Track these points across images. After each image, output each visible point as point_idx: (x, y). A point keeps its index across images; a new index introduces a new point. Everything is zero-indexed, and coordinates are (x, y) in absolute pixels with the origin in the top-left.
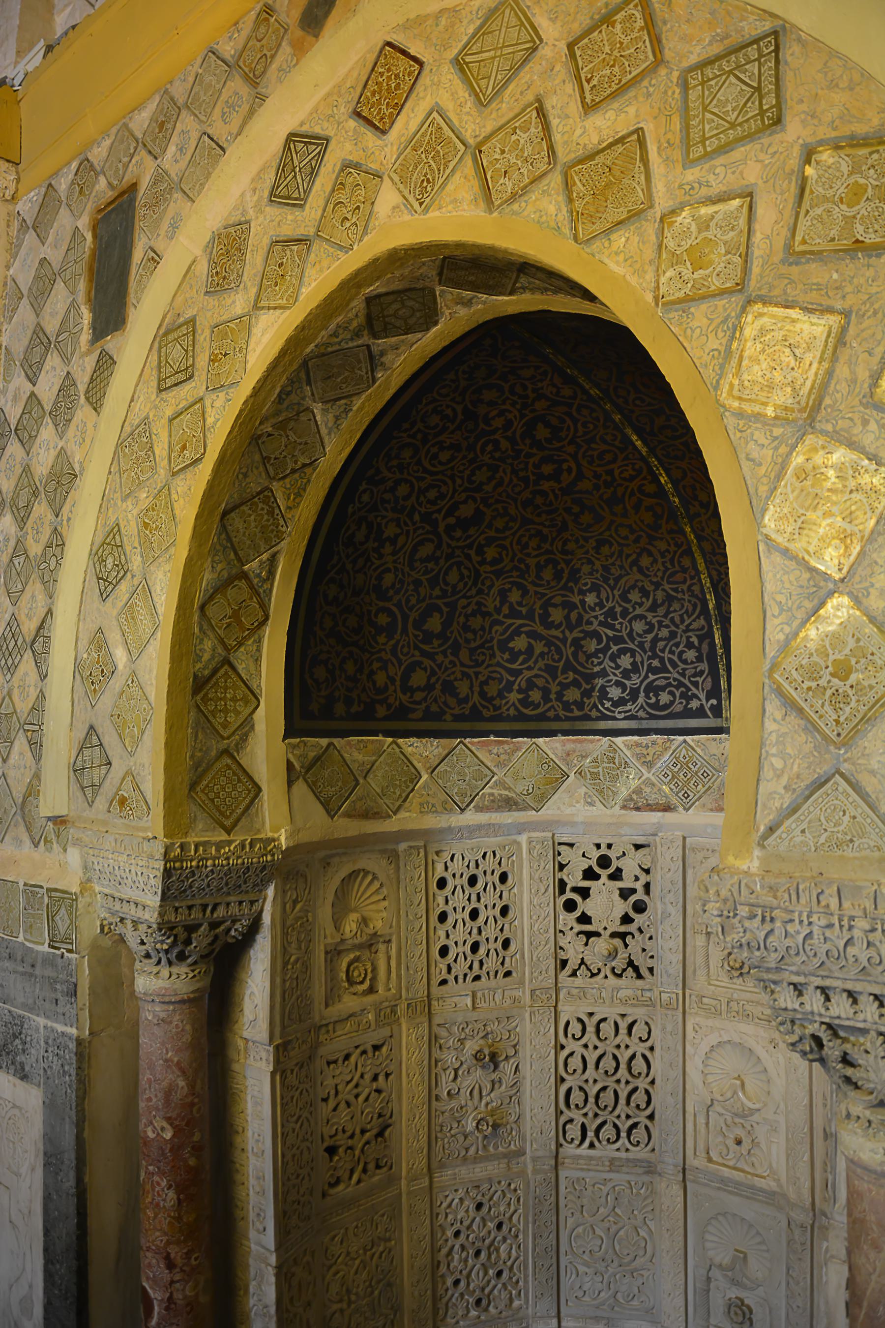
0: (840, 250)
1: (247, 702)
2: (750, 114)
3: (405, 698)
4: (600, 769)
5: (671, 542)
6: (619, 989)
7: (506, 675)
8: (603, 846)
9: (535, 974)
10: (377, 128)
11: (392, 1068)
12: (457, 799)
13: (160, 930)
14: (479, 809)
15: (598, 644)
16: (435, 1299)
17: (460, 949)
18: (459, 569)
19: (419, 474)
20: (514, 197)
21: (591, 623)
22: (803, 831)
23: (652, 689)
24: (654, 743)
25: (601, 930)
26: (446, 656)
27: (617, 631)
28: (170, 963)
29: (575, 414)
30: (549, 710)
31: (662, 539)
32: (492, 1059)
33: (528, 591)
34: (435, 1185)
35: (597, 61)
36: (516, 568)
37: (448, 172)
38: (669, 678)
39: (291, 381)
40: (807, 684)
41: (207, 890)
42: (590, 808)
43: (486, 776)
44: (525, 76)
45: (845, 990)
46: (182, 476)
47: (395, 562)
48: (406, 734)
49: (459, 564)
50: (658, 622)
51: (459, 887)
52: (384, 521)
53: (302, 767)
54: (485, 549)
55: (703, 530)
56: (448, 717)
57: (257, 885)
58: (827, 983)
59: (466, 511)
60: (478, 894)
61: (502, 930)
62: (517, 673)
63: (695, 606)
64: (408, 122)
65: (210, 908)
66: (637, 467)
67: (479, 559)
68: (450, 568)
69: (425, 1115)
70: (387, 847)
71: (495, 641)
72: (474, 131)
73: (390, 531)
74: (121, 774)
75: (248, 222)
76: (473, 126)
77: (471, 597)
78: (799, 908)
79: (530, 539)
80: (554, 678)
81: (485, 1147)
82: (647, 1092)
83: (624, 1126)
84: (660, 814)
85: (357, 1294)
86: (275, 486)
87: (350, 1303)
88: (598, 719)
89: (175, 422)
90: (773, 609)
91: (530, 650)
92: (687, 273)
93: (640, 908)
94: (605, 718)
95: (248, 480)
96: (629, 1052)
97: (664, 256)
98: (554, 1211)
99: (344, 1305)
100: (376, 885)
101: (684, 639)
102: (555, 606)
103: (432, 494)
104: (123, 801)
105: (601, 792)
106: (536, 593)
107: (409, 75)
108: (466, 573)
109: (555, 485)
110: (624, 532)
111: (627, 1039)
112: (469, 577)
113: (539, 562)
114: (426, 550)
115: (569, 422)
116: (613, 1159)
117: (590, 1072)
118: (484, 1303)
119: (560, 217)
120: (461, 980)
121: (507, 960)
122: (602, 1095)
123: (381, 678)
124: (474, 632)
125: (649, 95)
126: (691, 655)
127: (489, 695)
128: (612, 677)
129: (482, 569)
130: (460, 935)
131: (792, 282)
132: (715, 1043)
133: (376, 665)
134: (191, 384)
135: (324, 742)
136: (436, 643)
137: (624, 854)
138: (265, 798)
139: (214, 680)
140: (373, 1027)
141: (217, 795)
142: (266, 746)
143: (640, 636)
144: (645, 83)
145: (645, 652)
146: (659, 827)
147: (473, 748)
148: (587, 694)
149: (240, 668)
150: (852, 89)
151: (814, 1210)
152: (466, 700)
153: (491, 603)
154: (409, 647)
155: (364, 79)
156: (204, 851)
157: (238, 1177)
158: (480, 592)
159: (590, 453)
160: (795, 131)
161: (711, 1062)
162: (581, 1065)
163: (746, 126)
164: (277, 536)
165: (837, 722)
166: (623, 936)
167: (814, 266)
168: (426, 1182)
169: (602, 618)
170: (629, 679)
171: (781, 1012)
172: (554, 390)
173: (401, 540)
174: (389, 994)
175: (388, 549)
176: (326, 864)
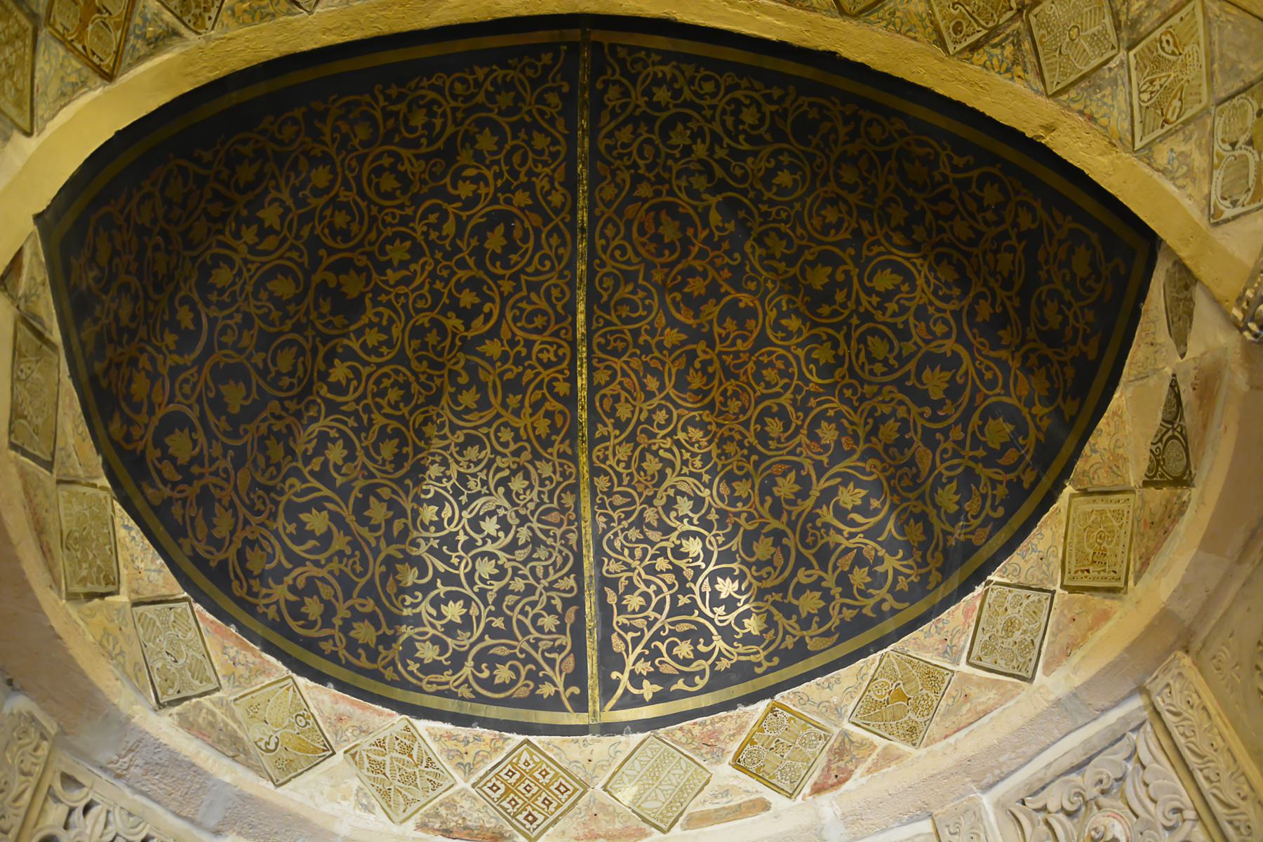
4: (387, 758)
5: (558, 469)
14: (187, 724)
15: (421, 576)
18: (296, 358)
19: (350, 176)
21: (418, 546)
23: (484, 657)
24: (477, 738)
26: (225, 456)
27: (452, 566)
29: (543, 236)
31: (548, 461)
33: (355, 458)
38: (514, 647)
42: (366, 815)
49: (301, 352)
50: (513, 568)
55: (604, 460)
56: (186, 543)
59: (353, 286)
62: (298, 561)
63: (566, 559)
66: (560, 352)
68: (290, 343)
71: (284, 499)
73: (270, 215)
79: (393, 386)
80: (348, 596)
88: (393, 683)
91: (326, 539)
94: (404, 684)
101: (544, 598)
102: (380, 499)
103: (341, 219)
105: (385, 794)
106: (364, 467)
108: (300, 372)
109: (462, 328)
110: (506, 435)
113: (386, 426)
114: (283, 288)
115: (531, 244)
124: (268, 459)
126: (549, 622)
127: (249, 566)
148: (387, 641)
152: (218, 544)
153: (304, 441)
154: (193, 389)
159: (523, 305)
169: (435, 544)
170: (454, 637)
172: (547, 187)
173: (270, 243)
175: (249, 235)
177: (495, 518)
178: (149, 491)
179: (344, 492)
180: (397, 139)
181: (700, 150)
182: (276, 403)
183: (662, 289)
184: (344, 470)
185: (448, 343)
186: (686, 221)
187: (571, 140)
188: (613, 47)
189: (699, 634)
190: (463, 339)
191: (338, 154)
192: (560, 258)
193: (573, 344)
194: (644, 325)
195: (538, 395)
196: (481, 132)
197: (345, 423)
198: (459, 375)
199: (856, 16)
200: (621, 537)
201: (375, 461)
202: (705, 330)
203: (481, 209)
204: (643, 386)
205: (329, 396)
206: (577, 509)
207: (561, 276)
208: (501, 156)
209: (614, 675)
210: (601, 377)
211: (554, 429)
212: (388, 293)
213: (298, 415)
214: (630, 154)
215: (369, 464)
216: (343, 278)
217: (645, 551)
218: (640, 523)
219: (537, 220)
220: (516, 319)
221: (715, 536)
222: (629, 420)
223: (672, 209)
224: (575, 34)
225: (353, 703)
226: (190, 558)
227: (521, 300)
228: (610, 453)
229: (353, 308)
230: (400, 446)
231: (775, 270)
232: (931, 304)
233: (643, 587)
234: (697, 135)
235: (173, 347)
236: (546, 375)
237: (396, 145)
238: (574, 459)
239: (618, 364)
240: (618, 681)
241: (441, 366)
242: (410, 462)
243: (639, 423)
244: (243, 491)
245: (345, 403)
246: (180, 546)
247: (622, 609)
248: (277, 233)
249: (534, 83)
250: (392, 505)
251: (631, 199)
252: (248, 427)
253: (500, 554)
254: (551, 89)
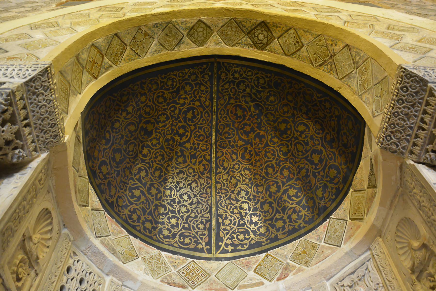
5: (206, 181)
7: (127, 202)
18: (134, 147)
19: (151, 98)
26: (114, 173)
30: (138, 226)
31: (203, 179)
47: (123, 121)
49: (135, 145)
55: (219, 179)
59: (150, 127)
62: (131, 203)
66: (207, 147)
68: (133, 143)
71: (129, 186)
73: (130, 109)
79: (159, 155)
100: (49, 236)
102: (154, 187)
103: (148, 110)
106: (150, 178)
108: (135, 149)
109: (179, 139)
110: (191, 171)
113: (157, 167)
114: (132, 128)
115: (199, 116)
124: (125, 174)
128: (166, 226)
129: (139, 154)
152: (112, 197)
153: (135, 170)
154: (108, 154)
159: (197, 133)
169: (169, 201)
172: (205, 100)
173: (129, 116)
175: (124, 114)
177: (187, 195)
178: (97, 181)
179: (145, 185)
180: (164, 88)
181: (248, 90)
182: (128, 159)
183: (238, 129)
184: (145, 179)
186: (244, 110)
187: (211, 87)
188: (223, 63)
189: (246, 232)
190: (180, 142)
191: (148, 92)
192: (208, 120)
193: (211, 145)
194: (232, 139)
195: (201, 159)
196: (186, 86)
197: (146, 165)
198: (178, 153)
199: (289, 56)
201: (154, 177)
202: (250, 141)
203: (186, 106)
204: (232, 157)
205: (142, 158)
206: (211, 194)
207: (208, 125)
208: (192, 92)
209: (220, 243)
210: (220, 154)
211: (205, 169)
212: (159, 129)
213: (133, 163)
214: (228, 91)
215: (152, 178)
216: (147, 125)
219: (201, 109)
220: (195, 137)
221: (252, 203)
222: (227, 167)
223: (240, 106)
224: (213, 60)
227: (196, 132)
228: (221, 177)
229: (150, 133)
230: (160, 173)
231: (270, 124)
232: (314, 135)
234: (247, 86)
235: (104, 143)
236: (203, 153)
237: (164, 90)
238: (211, 179)
239: (224, 151)
241: (173, 150)
243: (230, 168)
244: (118, 183)
245: (146, 160)
246: (103, 196)
248: (131, 114)
249: (201, 73)
250: (158, 189)
251: (228, 104)
252: (121, 165)
254: (206, 74)
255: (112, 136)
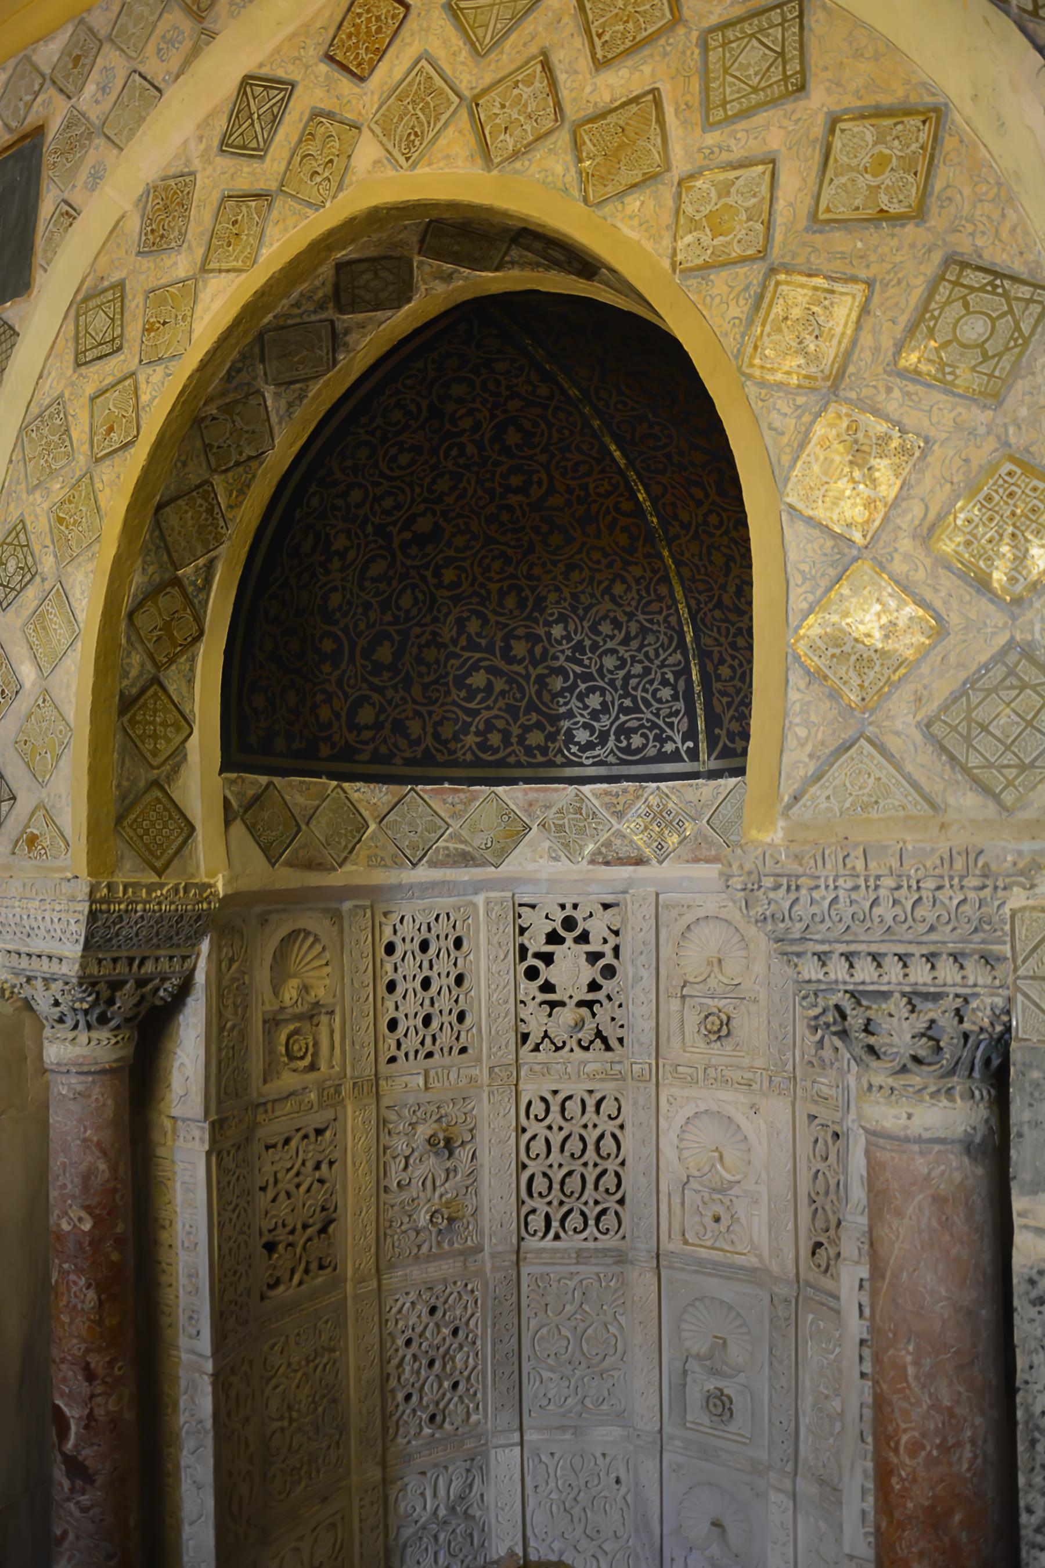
0: (865, 220)
1: (179, 729)
2: (774, 80)
3: (351, 737)
6: (585, 1063)
8: (569, 906)
9: (494, 1050)
10: (354, 74)
11: (336, 1155)
12: (408, 852)
13: (81, 985)
14: (432, 864)
15: (565, 681)
16: (385, 1417)
17: (411, 1022)
20: (516, 155)
21: (557, 659)
22: (828, 798)
24: (625, 791)
25: (566, 999)
26: (397, 691)
27: (586, 667)
28: (89, 1027)
31: (637, 564)
32: (446, 1145)
34: (384, 1288)
35: (609, 15)
36: (475, 594)
37: (439, 125)
39: (243, 356)
40: (831, 651)
41: (135, 940)
43: (440, 827)
44: (529, 26)
45: (869, 954)
46: (108, 462)
47: (343, 579)
48: (352, 778)
51: (409, 954)
52: (333, 532)
53: (240, 806)
54: (444, 571)
55: (682, 554)
56: (398, 761)
57: (190, 938)
58: (853, 948)
59: (424, 525)
60: (431, 961)
61: (456, 1001)
62: (474, 713)
64: (392, 69)
65: (137, 962)
66: (614, 481)
67: (436, 581)
69: (373, 1209)
70: (330, 903)
71: (451, 678)
72: (470, 82)
73: (340, 543)
74: (30, 809)
75: (193, 174)
76: (469, 77)
77: (425, 625)
78: (825, 873)
80: (516, 719)
81: (439, 1244)
82: (617, 1174)
83: (592, 1215)
84: (631, 868)
85: (299, 1411)
86: (216, 479)
87: (291, 1420)
88: (563, 765)
89: (98, 400)
90: (796, 578)
92: (706, 239)
93: (609, 972)
94: (571, 764)
95: (187, 469)
96: (597, 1132)
97: (682, 221)
98: (515, 1313)
99: (285, 1423)
100: (318, 948)
102: (518, 638)
103: (388, 503)
104: (32, 840)
105: (566, 845)
106: (498, 623)
107: (393, 18)
108: (420, 596)
110: (596, 555)
111: (594, 1117)
112: (424, 602)
113: (501, 588)
114: (377, 568)
115: (543, 426)
116: (580, 1250)
117: (555, 1157)
118: (439, 1418)
119: (568, 178)
120: (411, 1056)
121: (463, 1034)
122: (567, 1180)
123: (325, 713)
124: (428, 666)
125: (666, 54)
126: (666, 693)
130: (409, 1006)
131: (816, 250)
132: (691, 1114)
133: (319, 697)
134: (120, 357)
135: (264, 780)
136: (386, 675)
137: (591, 915)
138: (200, 838)
139: (142, 700)
140: (315, 1108)
141: (147, 832)
142: (200, 780)
143: (611, 672)
144: (662, 41)
145: (616, 691)
146: (631, 882)
147: (426, 797)
148: (552, 737)
149: (172, 689)
150: (877, 60)
151: (798, 1282)
152: (418, 742)
153: (447, 633)
154: (356, 679)
155: (339, 19)
156: (134, 893)
157: (164, 1279)
158: (435, 620)
159: (563, 463)
160: (820, 99)
161: (687, 1136)
162: (545, 1149)
163: (769, 91)
164: (215, 539)
165: (861, 686)
166: (589, 1004)
167: (837, 234)
168: (374, 1284)
169: (569, 653)
170: (598, 720)
171: (805, 985)
172: (530, 388)
173: (351, 555)
174: (332, 1071)
175: (336, 564)
176: (264, 920)
185: (519, 513)
200: (709, 615)
216: (413, 528)
217: (727, 629)
218: (719, 605)
225: (537, 790)
226: (405, 765)
233: (729, 661)
240: (719, 737)
242: (531, 600)
247: (718, 678)
253: (618, 648)
255: (340, 634)
